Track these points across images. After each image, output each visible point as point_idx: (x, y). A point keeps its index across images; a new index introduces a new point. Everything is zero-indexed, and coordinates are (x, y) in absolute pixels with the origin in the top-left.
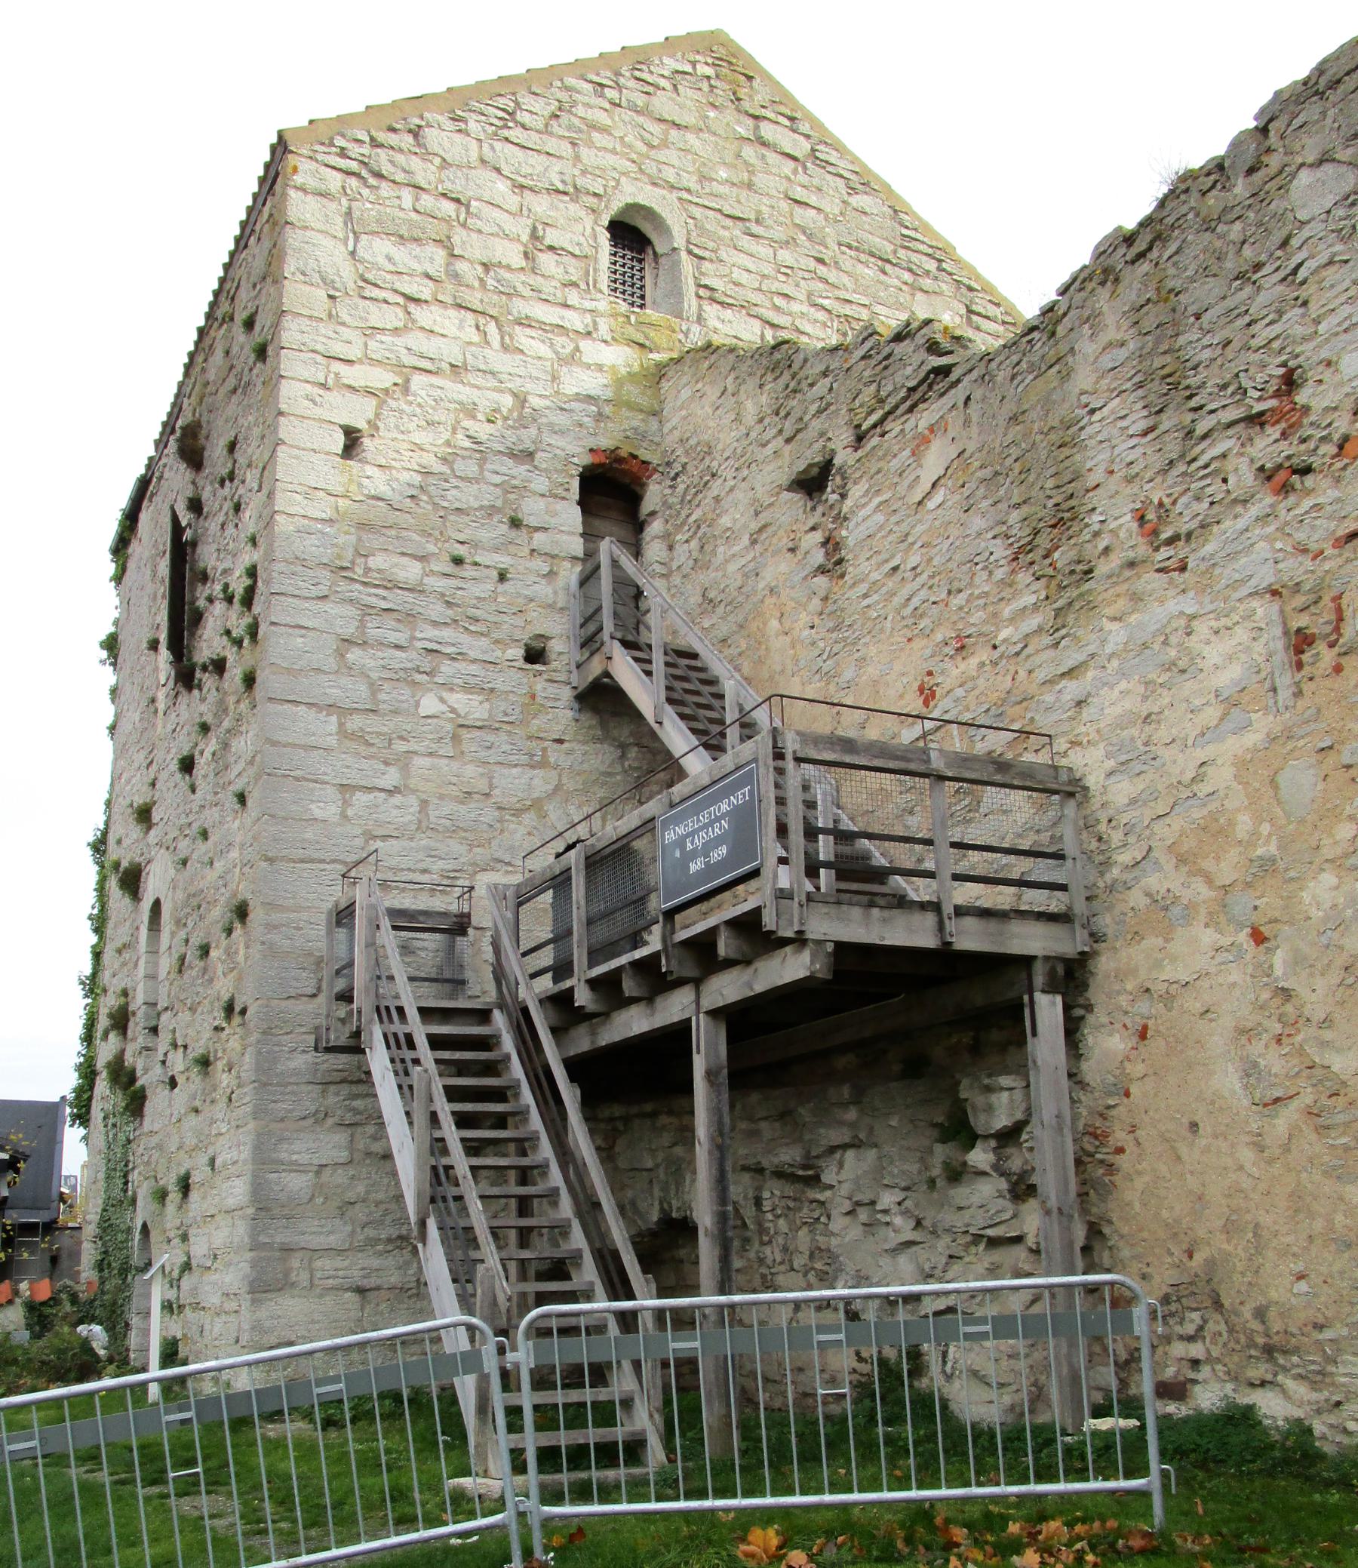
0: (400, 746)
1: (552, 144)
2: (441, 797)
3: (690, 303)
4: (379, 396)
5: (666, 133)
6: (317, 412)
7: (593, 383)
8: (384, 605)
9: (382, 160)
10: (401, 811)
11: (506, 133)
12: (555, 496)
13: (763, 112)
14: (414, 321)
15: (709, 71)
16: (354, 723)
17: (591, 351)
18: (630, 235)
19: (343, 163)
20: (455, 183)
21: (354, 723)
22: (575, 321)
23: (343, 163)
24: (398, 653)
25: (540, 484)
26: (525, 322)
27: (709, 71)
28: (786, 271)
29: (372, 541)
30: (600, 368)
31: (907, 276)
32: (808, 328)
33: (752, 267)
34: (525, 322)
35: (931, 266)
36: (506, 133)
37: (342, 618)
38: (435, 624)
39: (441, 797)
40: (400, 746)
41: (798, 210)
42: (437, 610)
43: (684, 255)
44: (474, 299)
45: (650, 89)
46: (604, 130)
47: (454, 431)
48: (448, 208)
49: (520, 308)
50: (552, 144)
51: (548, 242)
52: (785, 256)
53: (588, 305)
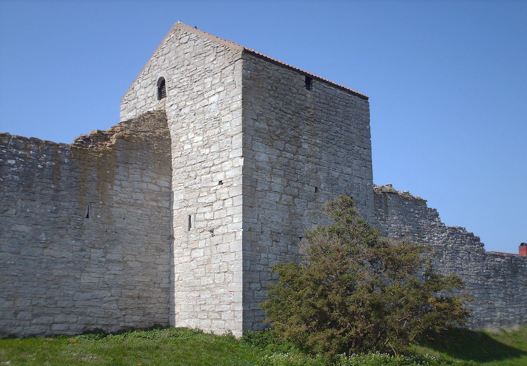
1: (150, 75)
13: (182, 36)
52: (182, 69)
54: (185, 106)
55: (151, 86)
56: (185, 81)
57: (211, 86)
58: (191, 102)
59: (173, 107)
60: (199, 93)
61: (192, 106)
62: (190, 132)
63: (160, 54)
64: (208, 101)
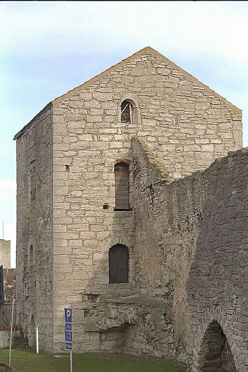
0: (78, 230)
1: (108, 90)
2: (87, 239)
3: (139, 121)
4: (72, 157)
5: (134, 79)
6: (61, 163)
7: (119, 145)
8: (75, 201)
9: (72, 104)
10: (78, 243)
11: (98, 90)
12: (110, 172)
13: (159, 66)
14: (79, 139)
15: (146, 59)
16: (69, 227)
17: (117, 137)
18: (126, 105)
19: (64, 106)
20: (87, 104)
21: (69, 227)
22: (113, 131)
23: (64, 106)
24: (78, 211)
25: (106, 170)
26: (102, 134)
27: (146, 59)
28: (163, 107)
29: (72, 189)
30: (119, 141)
31: (194, 99)
32: (168, 120)
33: (154, 107)
34: (102, 134)
35: (201, 95)
36: (98, 90)
37: (67, 206)
38: (85, 204)
39: (87, 239)
40: (78, 230)
41: (167, 89)
42: (84, 201)
43: (138, 109)
44: (92, 131)
45: (131, 69)
46: (120, 83)
47: (88, 162)
48: (86, 112)
49: (101, 131)
50: (108, 90)
51: (107, 114)
52: (163, 103)
53: (116, 126)
54: (168, 143)
55: (112, 104)
56: (168, 117)
57: (204, 135)
58: (177, 142)
59: (149, 139)
60: (188, 136)
61: (177, 145)
62: (175, 171)
63: (128, 73)
64: (201, 147)
